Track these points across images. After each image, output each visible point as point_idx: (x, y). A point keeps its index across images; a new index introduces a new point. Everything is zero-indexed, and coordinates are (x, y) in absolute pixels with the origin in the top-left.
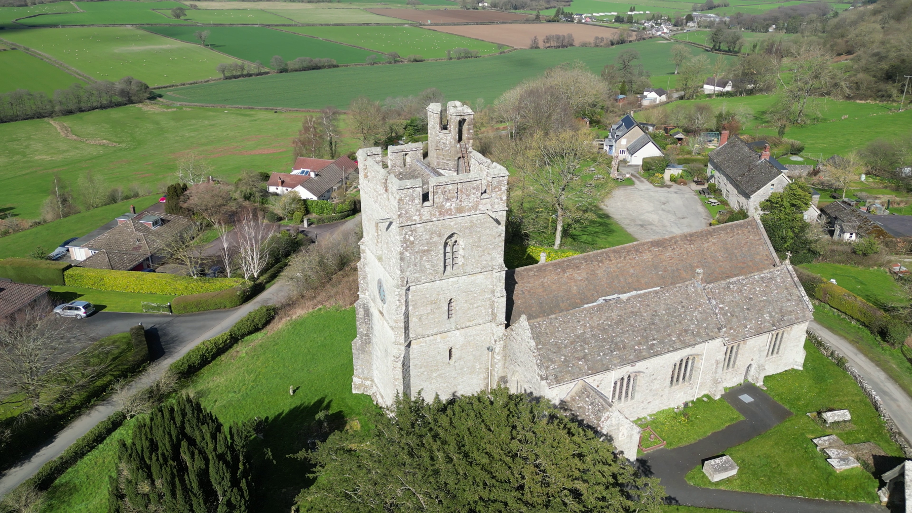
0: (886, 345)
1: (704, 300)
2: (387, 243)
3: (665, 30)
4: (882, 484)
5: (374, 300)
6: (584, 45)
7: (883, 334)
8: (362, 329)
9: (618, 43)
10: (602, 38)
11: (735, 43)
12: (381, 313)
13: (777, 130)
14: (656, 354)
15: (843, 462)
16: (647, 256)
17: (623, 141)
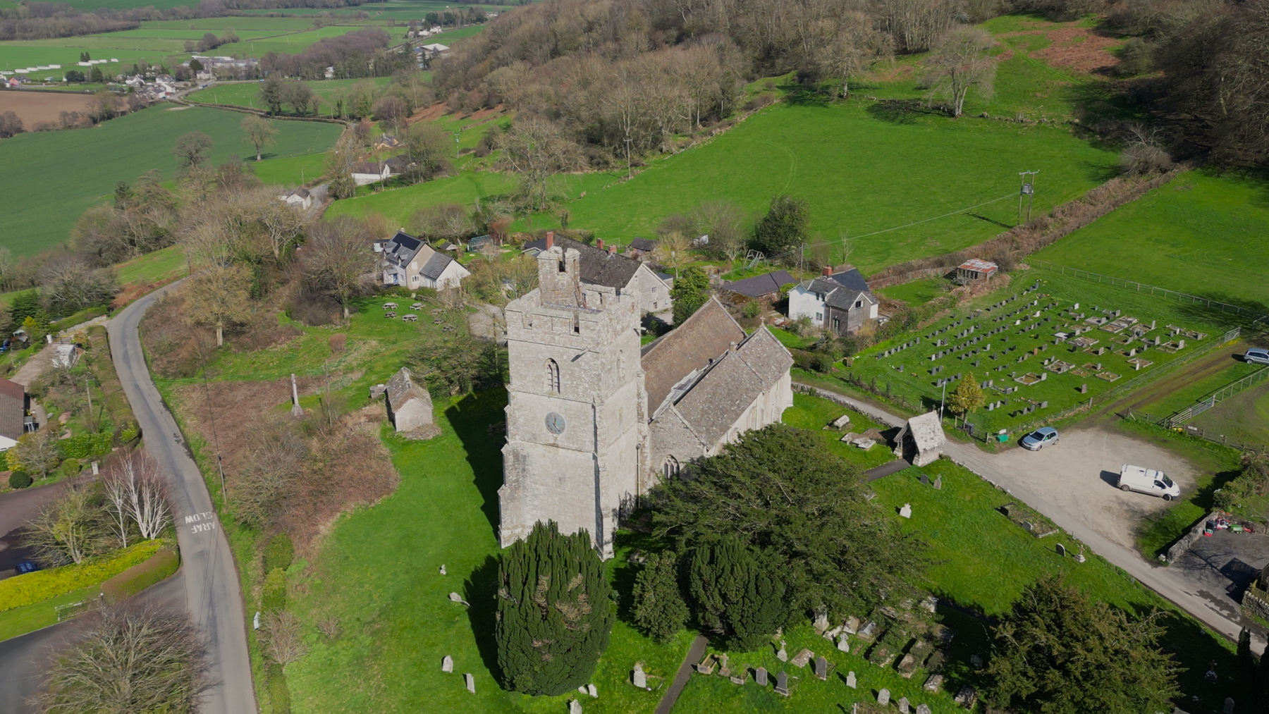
0: (821, 375)
1: (743, 365)
2: (572, 374)
3: (169, 89)
4: (893, 446)
5: (534, 439)
6: (43, 128)
7: (817, 367)
8: (510, 475)
9: (103, 118)
10: (74, 113)
11: (304, 102)
12: (553, 445)
13: (559, 222)
14: (743, 410)
15: (867, 444)
16: (676, 347)
17: (414, 266)
